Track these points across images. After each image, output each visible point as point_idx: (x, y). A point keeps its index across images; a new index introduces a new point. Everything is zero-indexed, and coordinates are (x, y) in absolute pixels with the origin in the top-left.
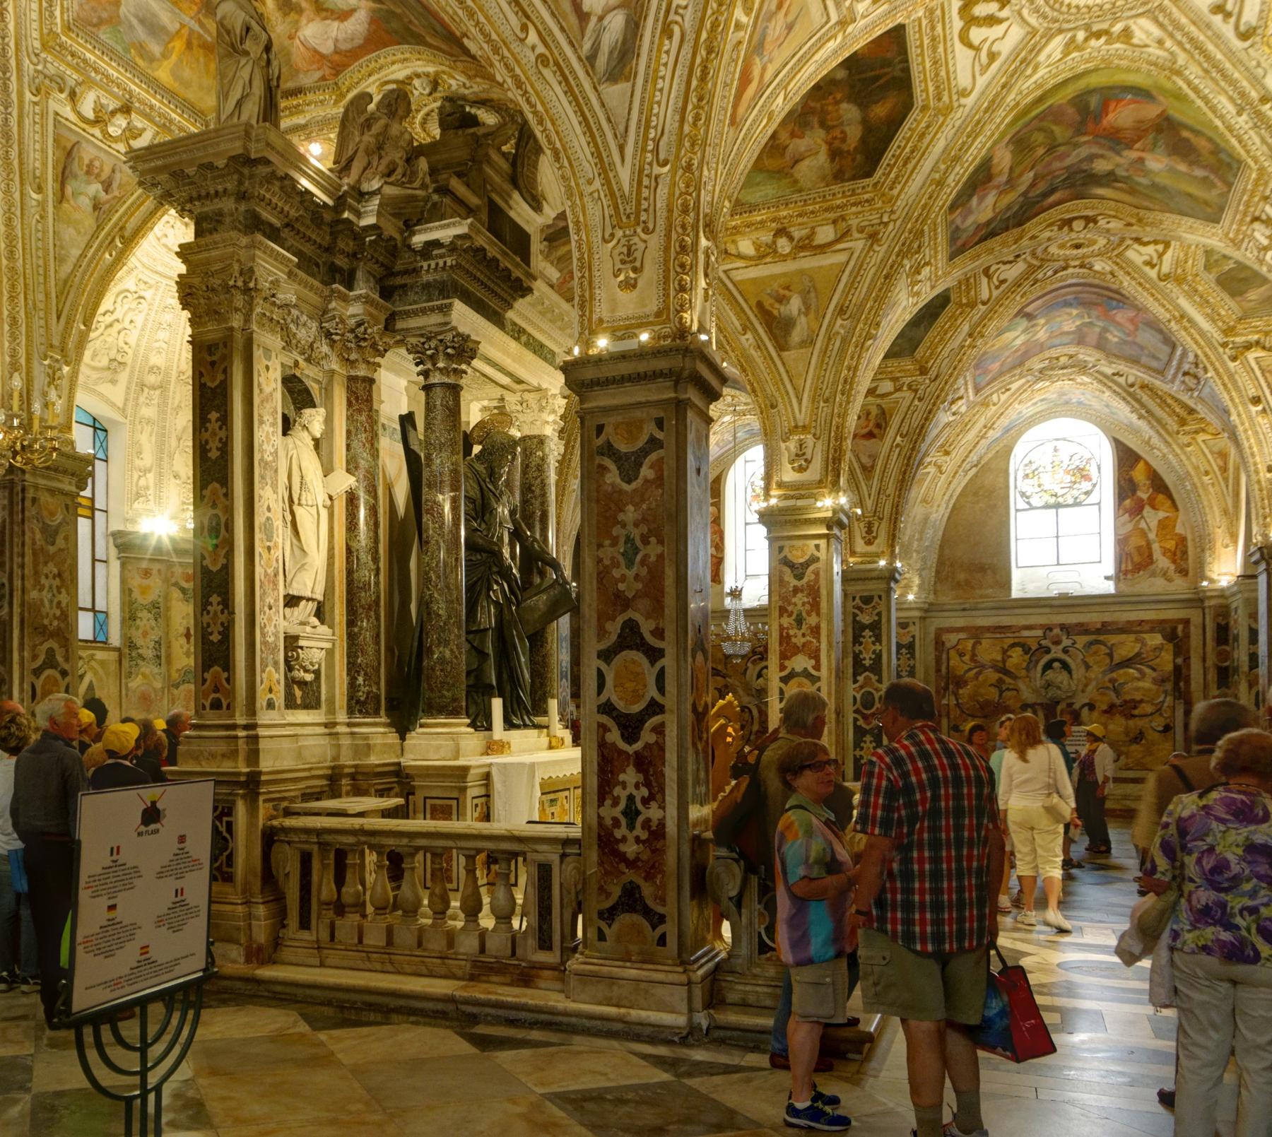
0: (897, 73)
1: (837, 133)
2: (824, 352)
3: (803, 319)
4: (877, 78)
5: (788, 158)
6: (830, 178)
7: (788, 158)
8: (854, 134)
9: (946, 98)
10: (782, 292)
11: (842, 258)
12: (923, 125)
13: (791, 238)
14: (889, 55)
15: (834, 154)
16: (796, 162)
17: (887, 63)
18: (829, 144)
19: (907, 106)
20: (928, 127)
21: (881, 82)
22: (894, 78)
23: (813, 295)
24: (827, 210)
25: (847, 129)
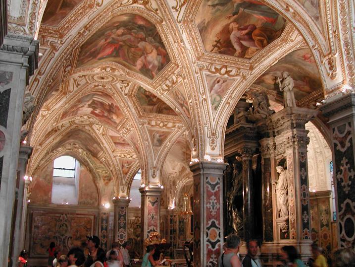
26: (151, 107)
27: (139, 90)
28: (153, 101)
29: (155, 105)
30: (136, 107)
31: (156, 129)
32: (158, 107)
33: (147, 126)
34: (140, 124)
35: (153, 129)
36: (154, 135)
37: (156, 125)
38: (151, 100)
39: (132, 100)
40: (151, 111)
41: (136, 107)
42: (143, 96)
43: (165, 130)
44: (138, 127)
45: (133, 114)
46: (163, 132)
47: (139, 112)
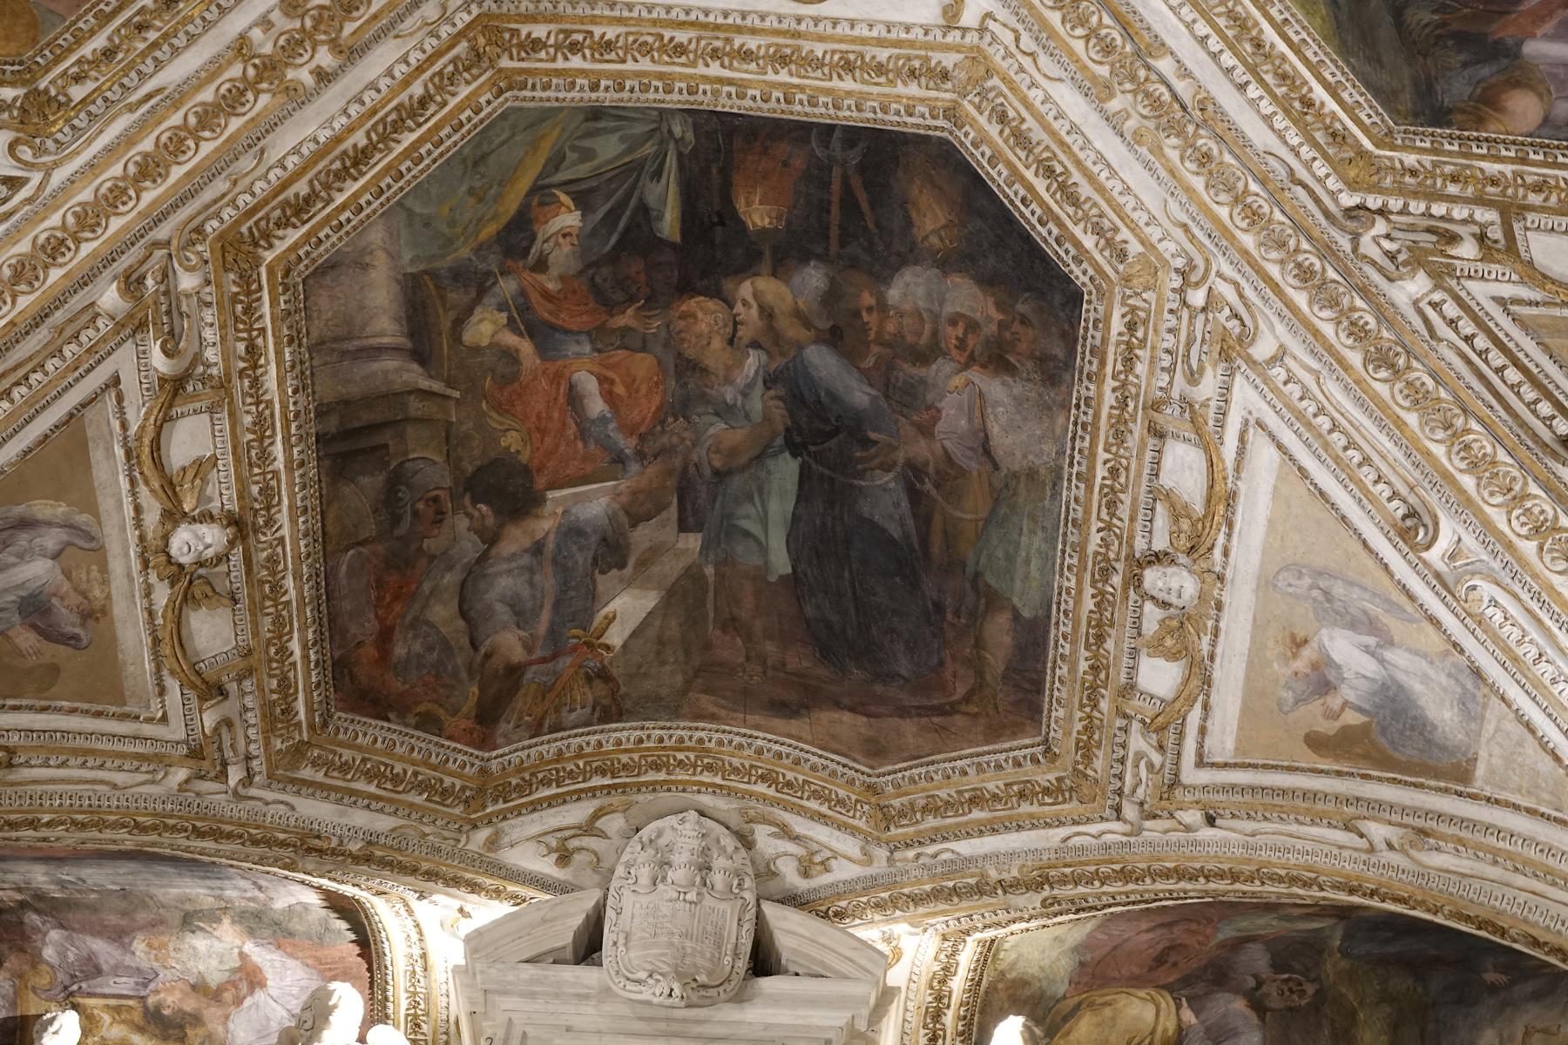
0: (854, 157)
1: (953, 333)
2: (1512, 661)
3: (1397, 657)
4: (849, 204)
5: (974, 466)
6: (1050, 395)
7: (974, 466)
8: (963, 296)
9: (949, 60)
10: (1300, 665)
11: (1264, 457)
12: (993, 130)
13: (1157, 558)
14: (798, 163)
15: (998, 360)
16: (986, 450)
17: (818, 175)
18: (971, 361)
19: (945, 161)
20: (1003, 118)
21: (862, 197)
22: (862, 168)
23: (1338, 590)
24: (1120, 436)
25: (949, 309)
26: (385, 326)
27: (596, 113)
28: (459, 324)
29: (421, 355)
30: (361, 158)
31: (120, 502)
32: (396, 397)
33: (129, 383)
34: (132, 283)
35: (110, 470)
36: (26, 524)
37: (169, 488)
38: (481, 286)
39: (446, 82)
40: (326, 347)
41: (361, 158)
42: (524, 184)
43: (132, 606)
44: (86, 279)
45: (255, 138)
46: (94, 614)
47: (299, 209)
